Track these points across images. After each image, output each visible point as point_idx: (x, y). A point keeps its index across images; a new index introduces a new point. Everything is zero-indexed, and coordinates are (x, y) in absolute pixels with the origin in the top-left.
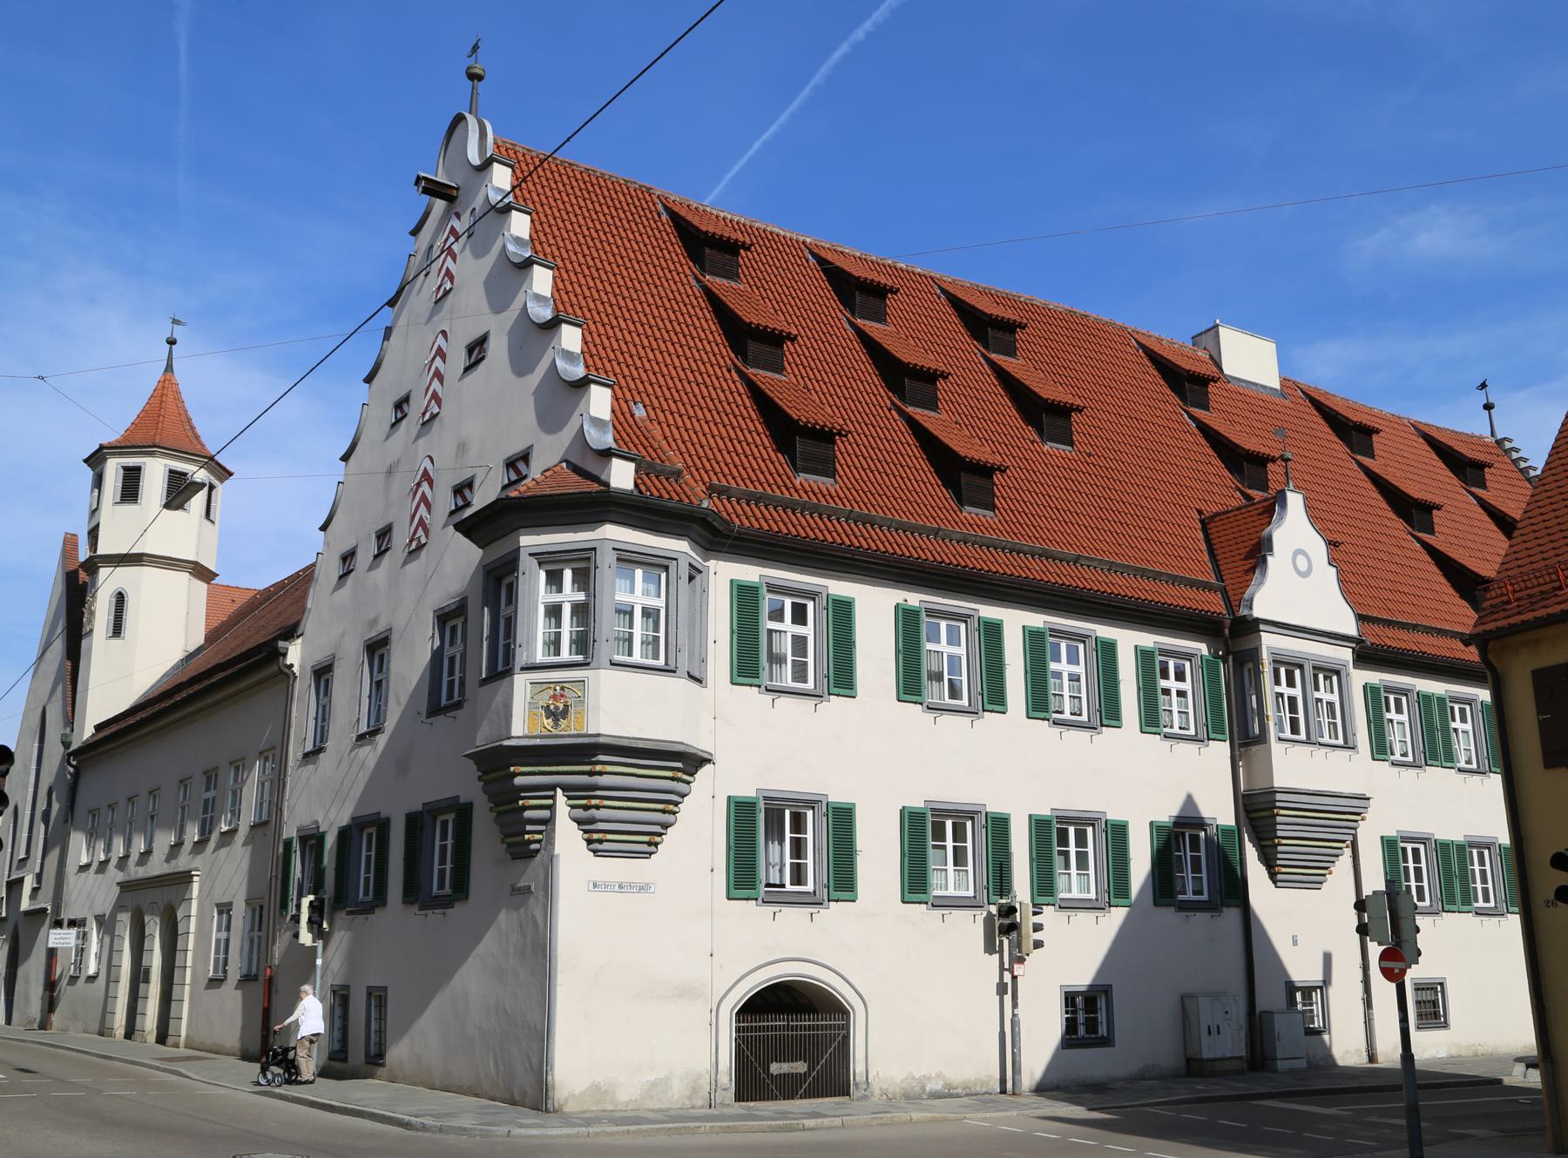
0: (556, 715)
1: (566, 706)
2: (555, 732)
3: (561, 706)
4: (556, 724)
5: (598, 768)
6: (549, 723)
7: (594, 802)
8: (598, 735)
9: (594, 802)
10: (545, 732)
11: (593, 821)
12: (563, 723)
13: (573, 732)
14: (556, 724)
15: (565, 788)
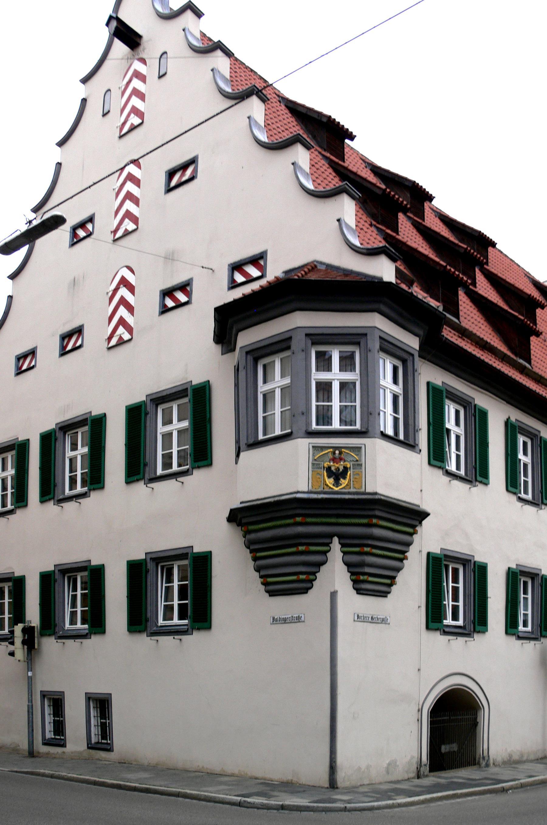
0: (338, 476)
1: (346, 469)
2: (336, 489)
3: (341, 468)
4: (337, 483)
5: (375, 521)
6: (330, 482)
7: (367, 549)
8: (376, 494)
9: (367, 549)
10: (327, 489)
11: (363, 564)
12: (344, 482)
13: (352, 490)
14: (337, 483)
15: (340, 537)
